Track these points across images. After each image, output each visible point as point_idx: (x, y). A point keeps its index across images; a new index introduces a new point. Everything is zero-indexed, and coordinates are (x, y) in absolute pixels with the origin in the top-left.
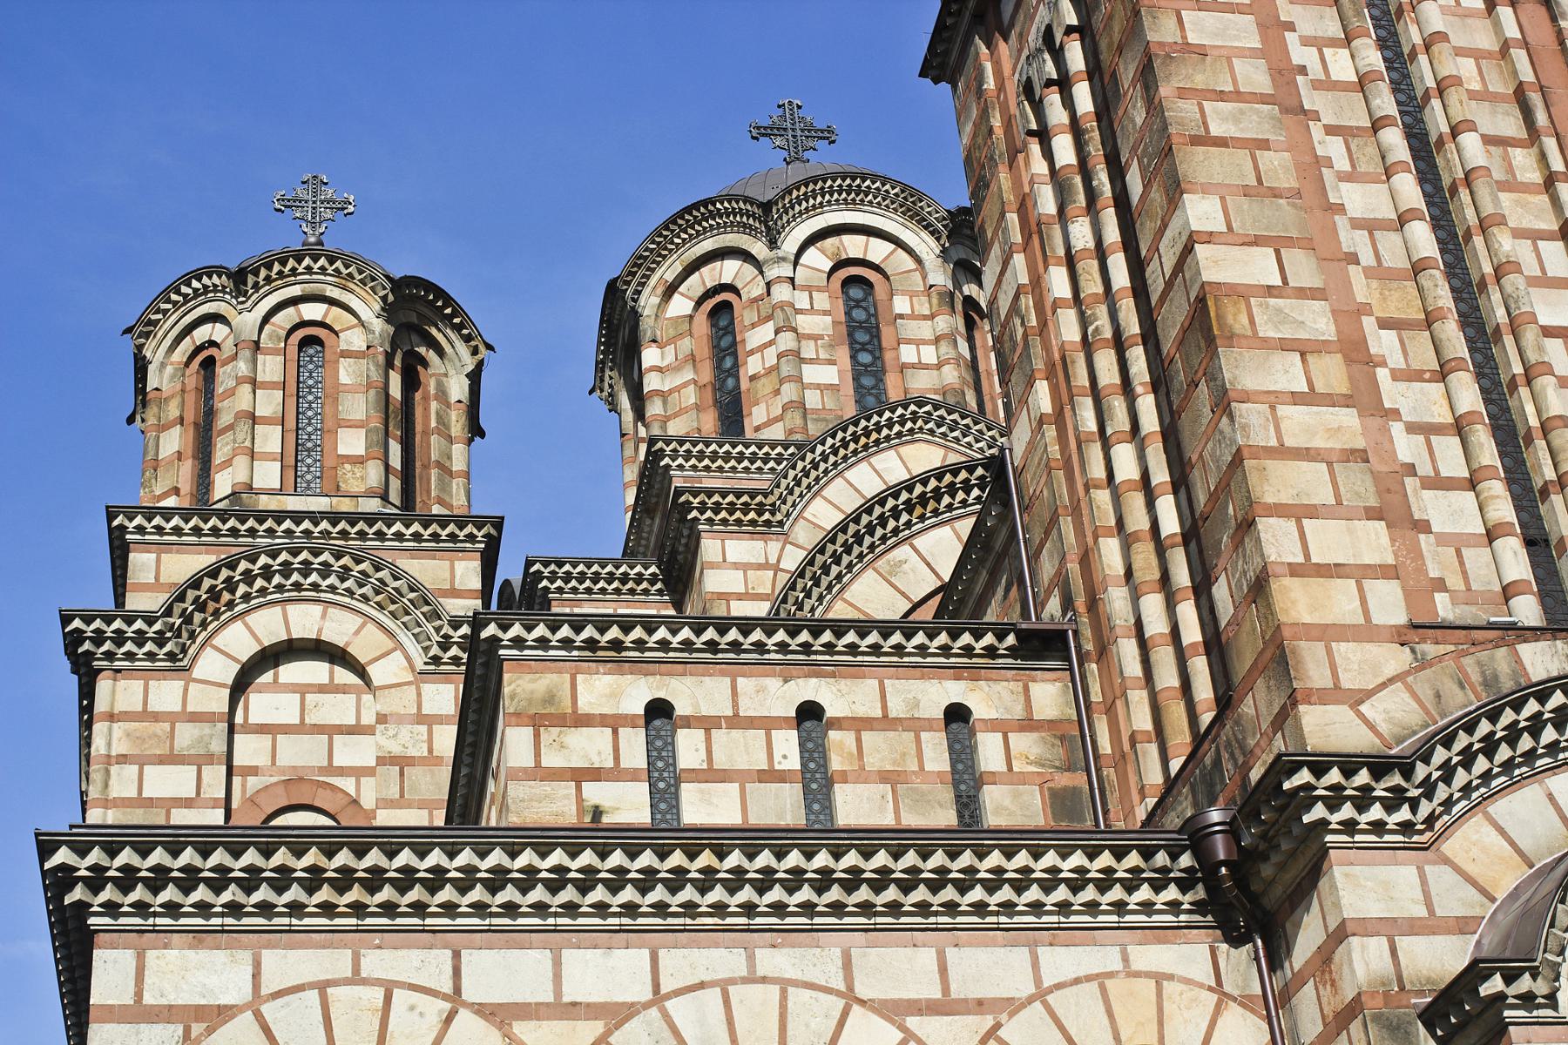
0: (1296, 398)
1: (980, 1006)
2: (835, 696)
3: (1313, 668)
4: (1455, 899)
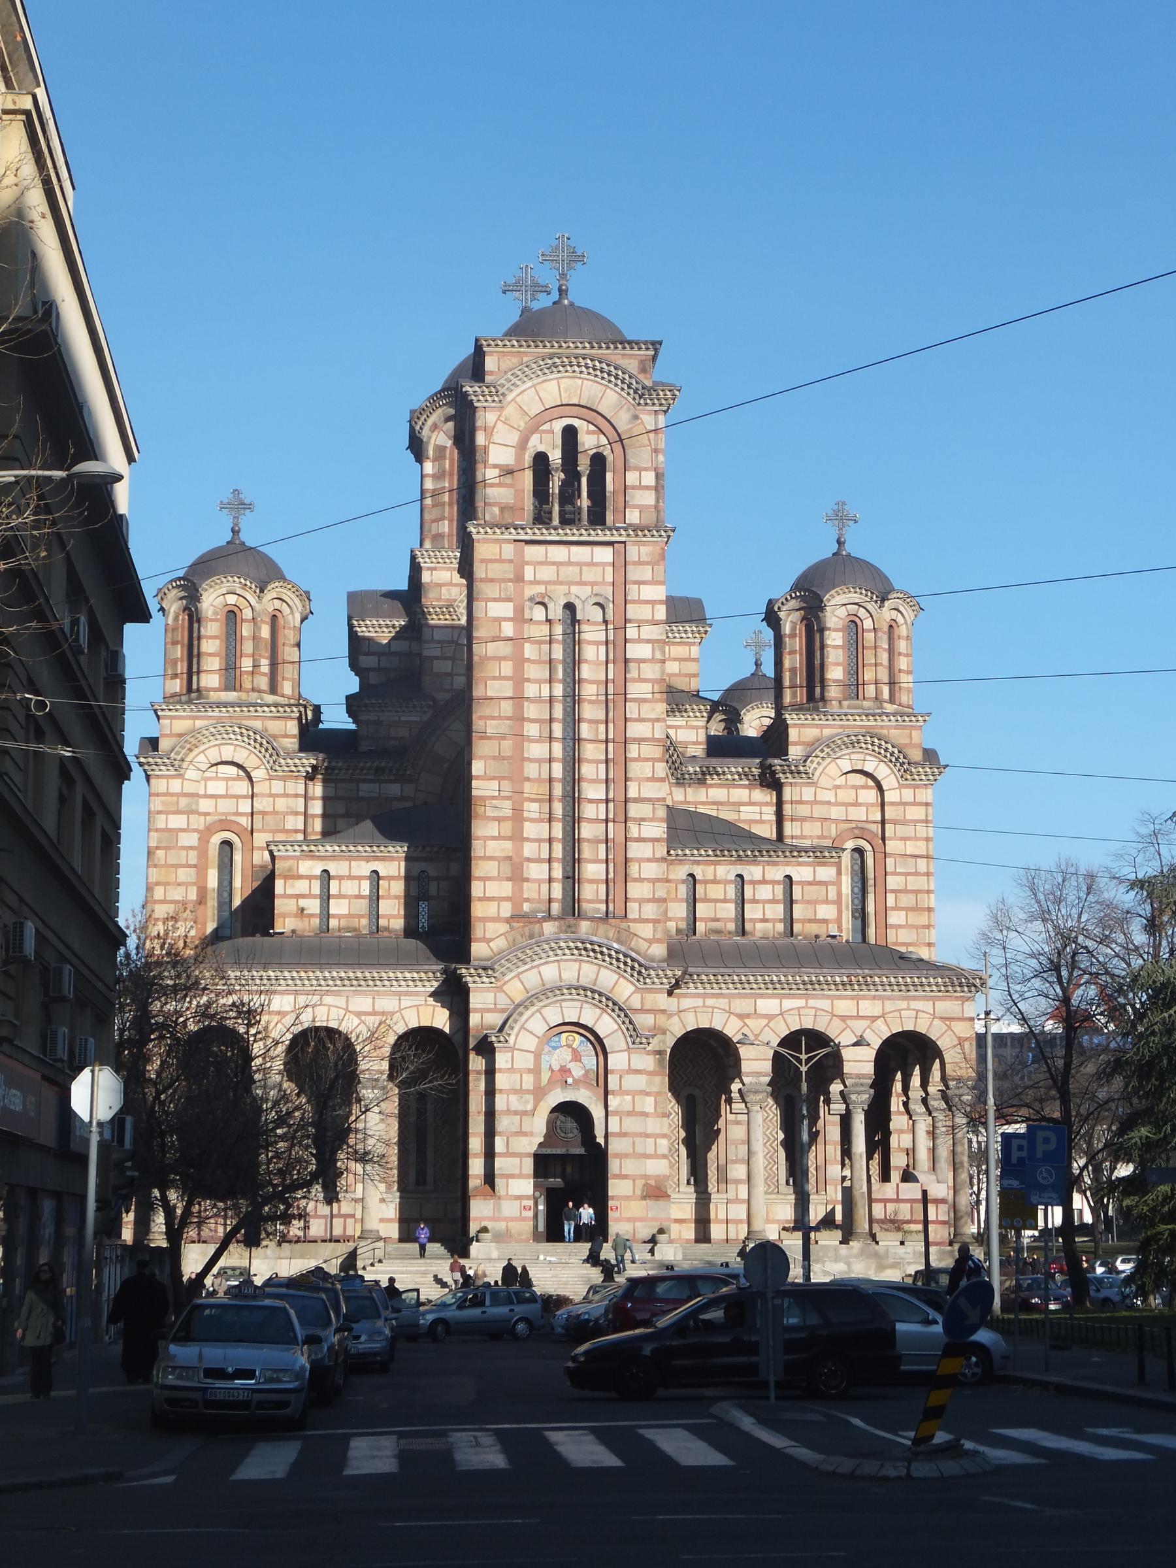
0: (494, 838)
3: (477, 930)
4: (503, 1001)
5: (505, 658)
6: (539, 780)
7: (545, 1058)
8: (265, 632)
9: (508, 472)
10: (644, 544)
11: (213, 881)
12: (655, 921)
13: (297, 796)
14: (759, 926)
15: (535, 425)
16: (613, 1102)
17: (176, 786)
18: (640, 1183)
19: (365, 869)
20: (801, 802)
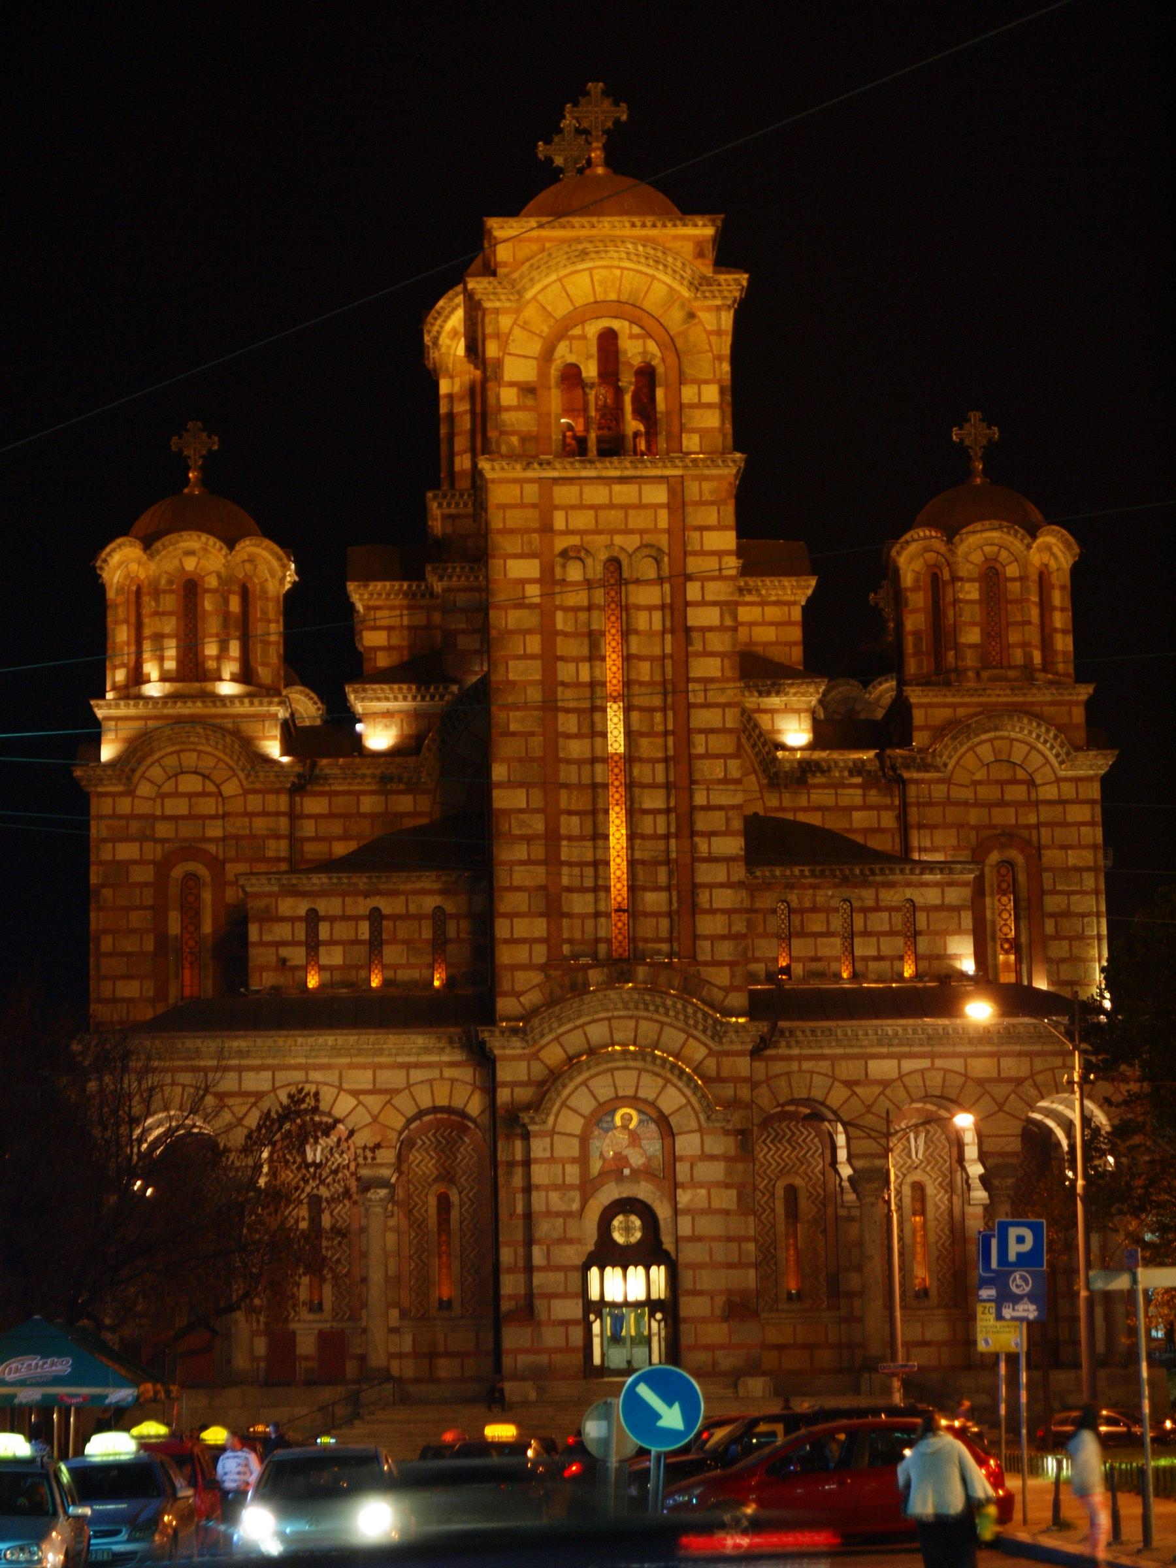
1: (385, 1091)
2: (386, 906)
4: (538, 1071)
5: (530, 631)
6: (580, 786)
7: (595, 1144)
8: (235, 605)
9: (528, 390)
10: (707, 478)
11: (174, 925)
12: (732, 964)
13: (278, 814)
14: (873, 965)
15: (562, 331)
16: (684, 1198)
17: (125, 806)
18: (720, 1300)
19: (363, 906)
20: (931, 804)
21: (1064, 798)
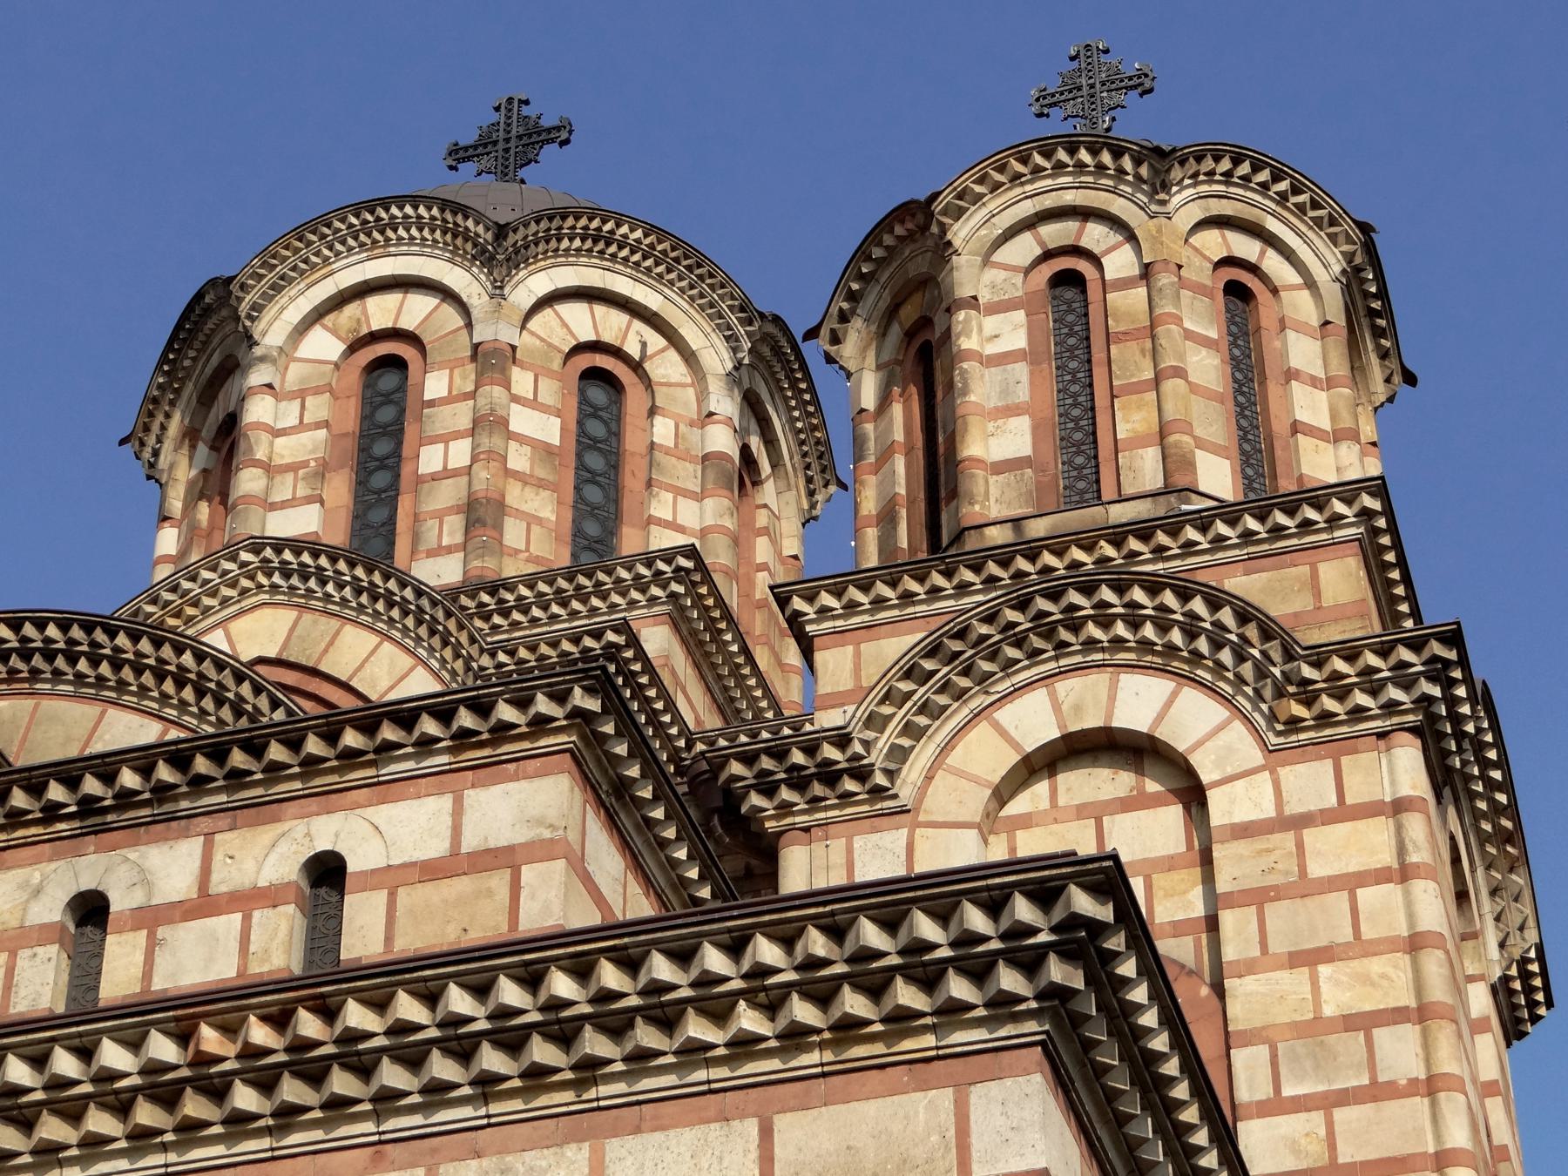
21: (1293, 808)
